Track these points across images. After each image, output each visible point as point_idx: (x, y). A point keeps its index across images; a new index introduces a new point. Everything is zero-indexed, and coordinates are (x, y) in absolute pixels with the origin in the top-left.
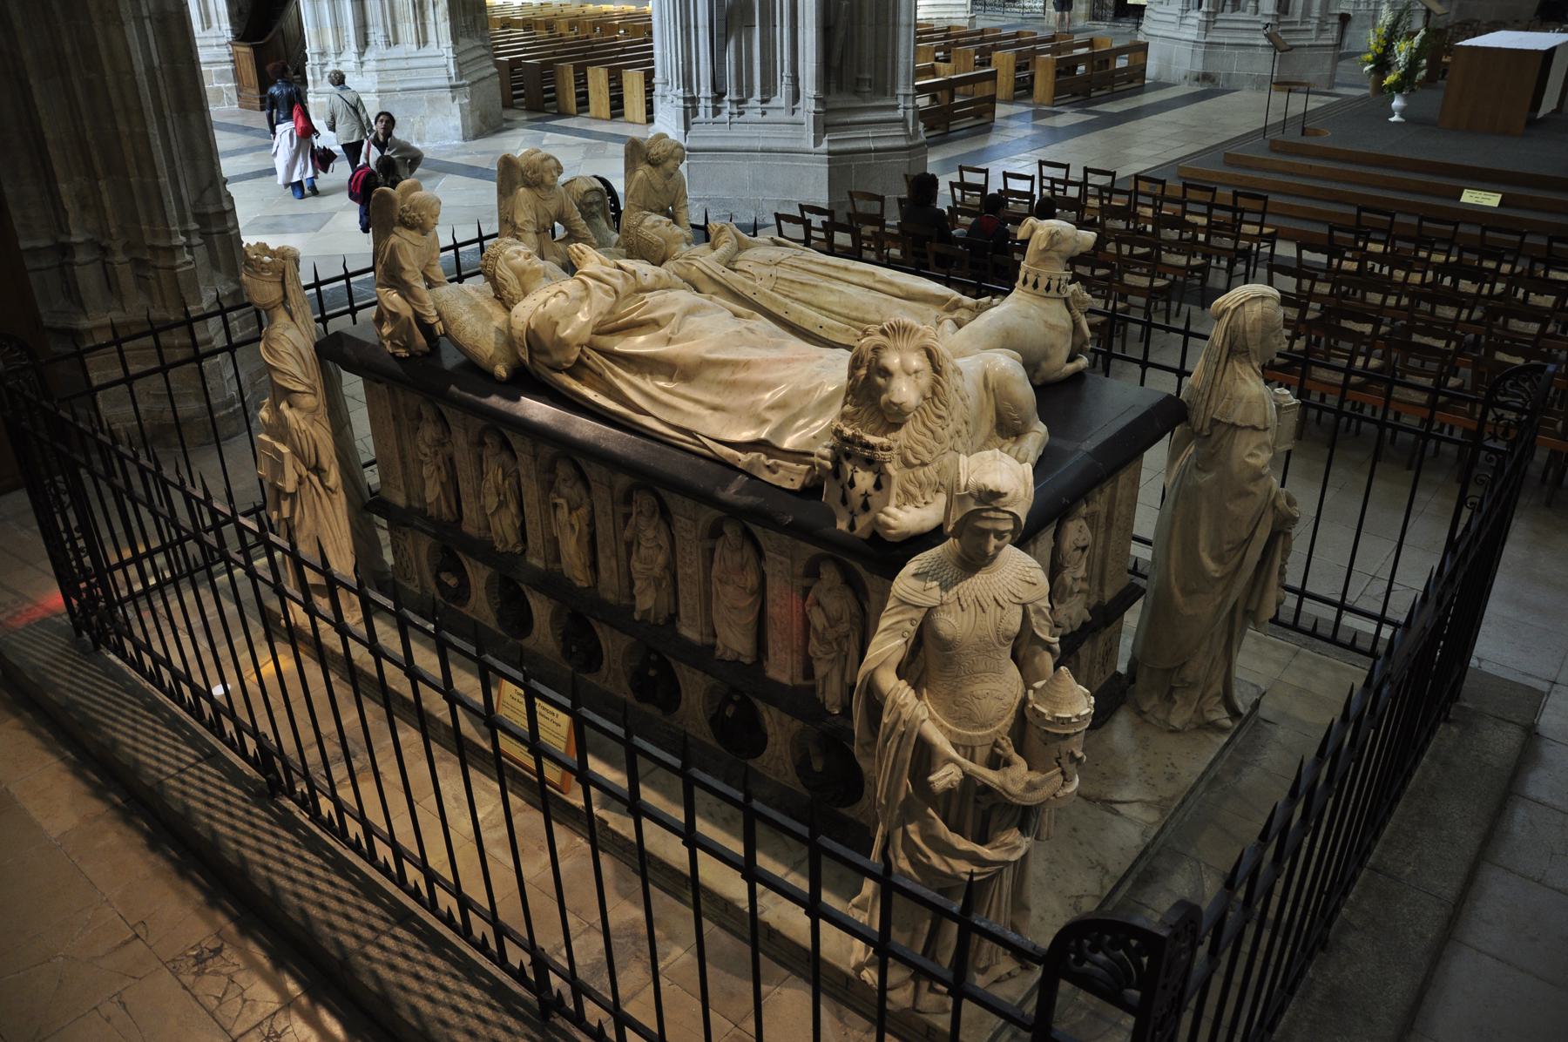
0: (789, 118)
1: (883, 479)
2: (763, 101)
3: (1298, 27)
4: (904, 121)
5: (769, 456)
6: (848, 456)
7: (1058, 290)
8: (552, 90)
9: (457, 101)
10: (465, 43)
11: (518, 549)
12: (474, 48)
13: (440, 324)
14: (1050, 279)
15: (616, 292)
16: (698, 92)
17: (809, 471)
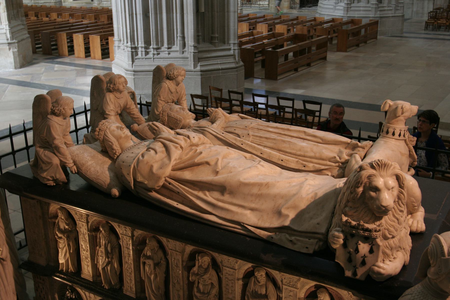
0: (181, 56)
1: (374, 248)
2: (169, 48)
3: (386, 8)
4: (233, 56)
5: (291, 235)
6: (353, 235)
7: (404, 136)
8: (56, 45)
9: (11, 50)
10: (15, 23)
11: (118, 287)
12: (18, 25)
13: (75, 167)
14: (401, 130)
15: (181, 147)
16: (138, 44)
17: (317, 242)
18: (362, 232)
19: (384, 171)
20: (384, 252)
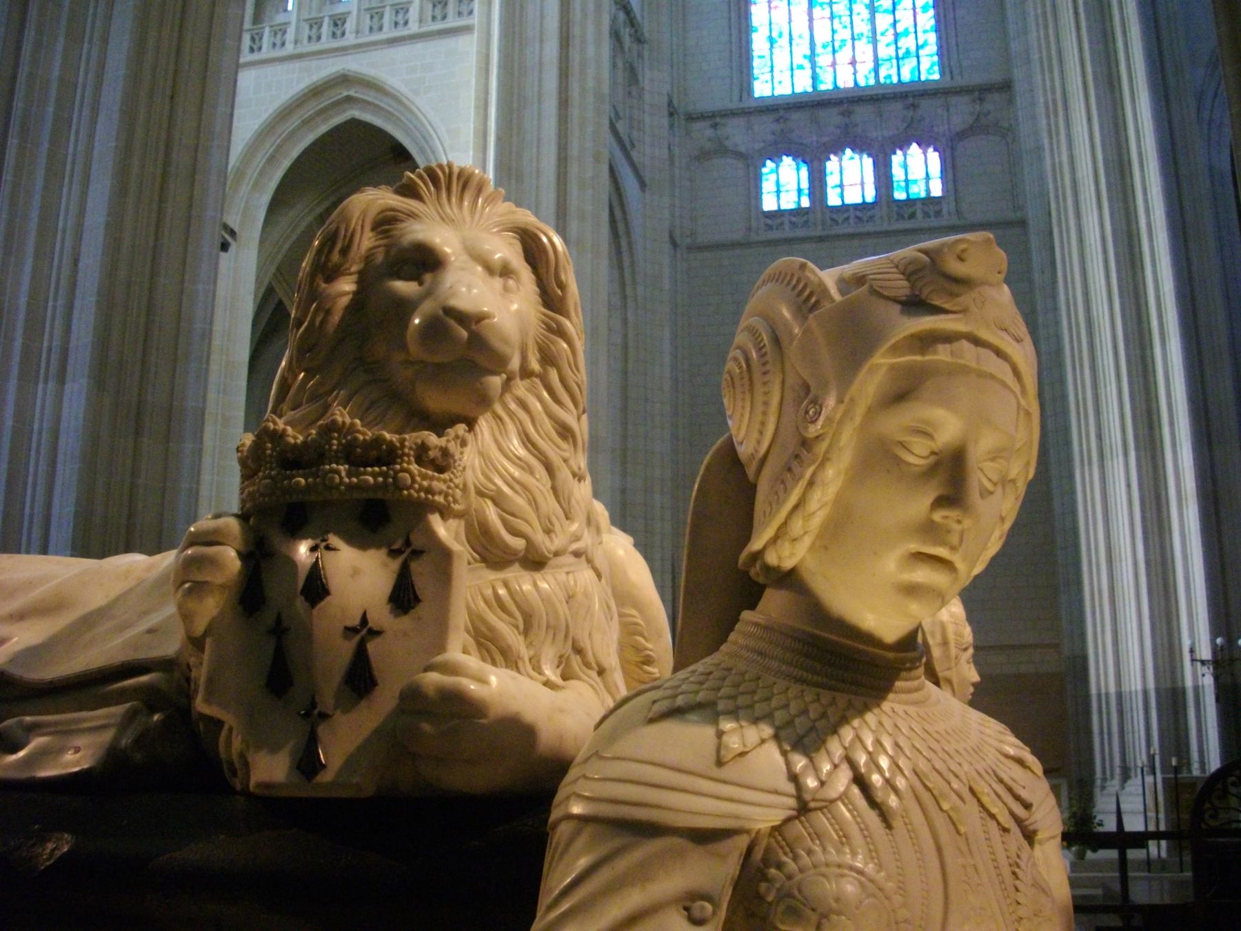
17: (131, 717)
18: (343, 468)
19: (461, 199)
20: (483, 629)
